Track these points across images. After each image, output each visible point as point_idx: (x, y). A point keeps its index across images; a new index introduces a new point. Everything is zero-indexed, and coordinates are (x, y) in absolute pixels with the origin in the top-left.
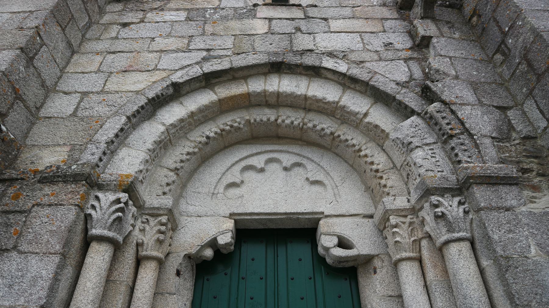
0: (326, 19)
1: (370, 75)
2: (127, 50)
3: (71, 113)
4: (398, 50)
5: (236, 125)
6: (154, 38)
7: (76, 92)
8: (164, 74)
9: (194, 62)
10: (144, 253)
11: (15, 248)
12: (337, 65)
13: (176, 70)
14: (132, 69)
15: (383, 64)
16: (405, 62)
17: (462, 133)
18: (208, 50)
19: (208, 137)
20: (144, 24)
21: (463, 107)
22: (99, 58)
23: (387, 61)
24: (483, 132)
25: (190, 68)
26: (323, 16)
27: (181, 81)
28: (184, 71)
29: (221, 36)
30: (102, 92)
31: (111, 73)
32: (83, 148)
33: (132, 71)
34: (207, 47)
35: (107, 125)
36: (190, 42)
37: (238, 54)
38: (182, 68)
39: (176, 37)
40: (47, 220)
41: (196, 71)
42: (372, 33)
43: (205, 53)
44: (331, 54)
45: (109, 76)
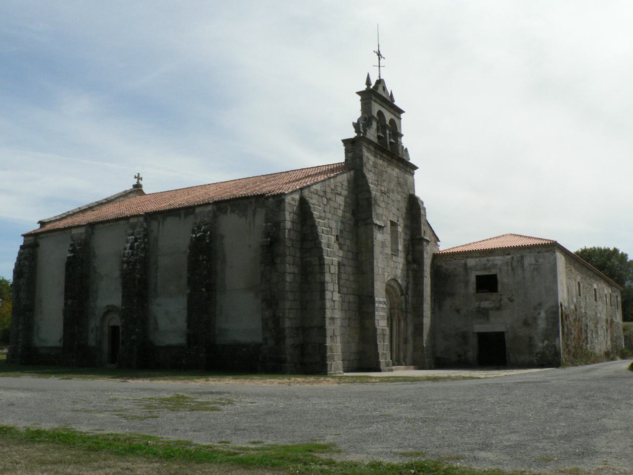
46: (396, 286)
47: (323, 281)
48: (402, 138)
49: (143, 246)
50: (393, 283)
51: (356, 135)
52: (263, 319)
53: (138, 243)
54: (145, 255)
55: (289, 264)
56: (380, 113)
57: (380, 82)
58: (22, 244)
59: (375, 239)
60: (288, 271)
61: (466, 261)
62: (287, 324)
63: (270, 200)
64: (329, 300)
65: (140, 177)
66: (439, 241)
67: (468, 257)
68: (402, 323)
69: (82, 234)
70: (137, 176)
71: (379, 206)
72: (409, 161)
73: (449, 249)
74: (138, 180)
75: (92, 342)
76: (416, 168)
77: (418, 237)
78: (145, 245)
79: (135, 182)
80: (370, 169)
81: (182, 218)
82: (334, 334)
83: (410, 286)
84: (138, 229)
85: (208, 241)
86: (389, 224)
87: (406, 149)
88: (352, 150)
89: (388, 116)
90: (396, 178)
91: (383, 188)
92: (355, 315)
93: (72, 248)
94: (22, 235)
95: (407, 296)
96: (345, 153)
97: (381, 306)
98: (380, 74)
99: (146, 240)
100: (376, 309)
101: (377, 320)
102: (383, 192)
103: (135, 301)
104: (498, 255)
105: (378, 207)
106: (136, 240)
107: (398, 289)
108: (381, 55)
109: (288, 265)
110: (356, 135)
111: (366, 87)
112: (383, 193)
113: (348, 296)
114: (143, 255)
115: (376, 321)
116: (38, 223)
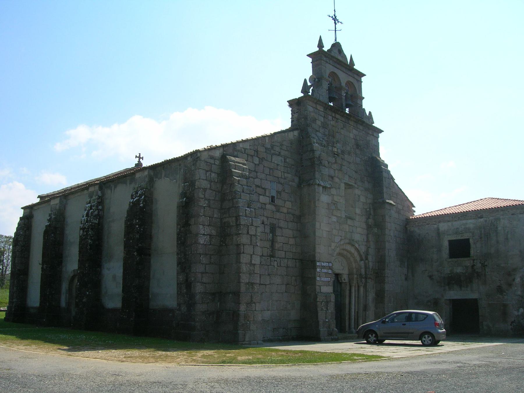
18: (341, 236)
46: (353, 250)
47: (239, 243)
48: (363, 101)
49: (96, 213)
50: (349, 247)
51: (302, 95)
52: (178, 284)
53: (92, 210)
54: (99, 222)
55: (204, 225)
56: (333, 75)
57: (337, 46)
58: (22, 216)
59: (318, 200)
60: (202, 232)
61: (438, 226)
62: (199, 288)
63: (189, 158)
64: (246, 264)
65: (141, 156)
66: (414, 207)
67: (440, 222)
68: (362, 289)
69: (57, 204)
70: (138, 156)
71: (325, 167)
72: (373, 125)
73: (423, 214)
74: (139, 159)
75: (63, 304)
76: (381, 131)
77: (381, 201)
78: (98, 212)
79: (136, 161)
80: (318, 130)
81: (128, 184)
82: (252, 301)
83: (372, 251)
84: (94, 198)
85: (141, 205)
86: (343, 186)
87: (370, 113)
88: (298, 111)
89: (344, 78)
90: (353, 141)
91: (335, 150)
92: (296, 280)
93: (96, 222)
94: (22, 208)
96: (292, 114)
97: (325, 271)
98: (336, 38)
99: (100, 207)
101: (320, 286)
102: (336, 153)
103: (87, 265)
104: (471, 219)
105: (324, 167)
106: (91, 208)
107: (356, 254)
108: (337, 20)
109: (201, 227)
110: (302, 95)
111: (317, 49)
112: (335, 155)
113: (286, 261)
114: (97, 222)
115: (317, 287)
116: (38, 198)
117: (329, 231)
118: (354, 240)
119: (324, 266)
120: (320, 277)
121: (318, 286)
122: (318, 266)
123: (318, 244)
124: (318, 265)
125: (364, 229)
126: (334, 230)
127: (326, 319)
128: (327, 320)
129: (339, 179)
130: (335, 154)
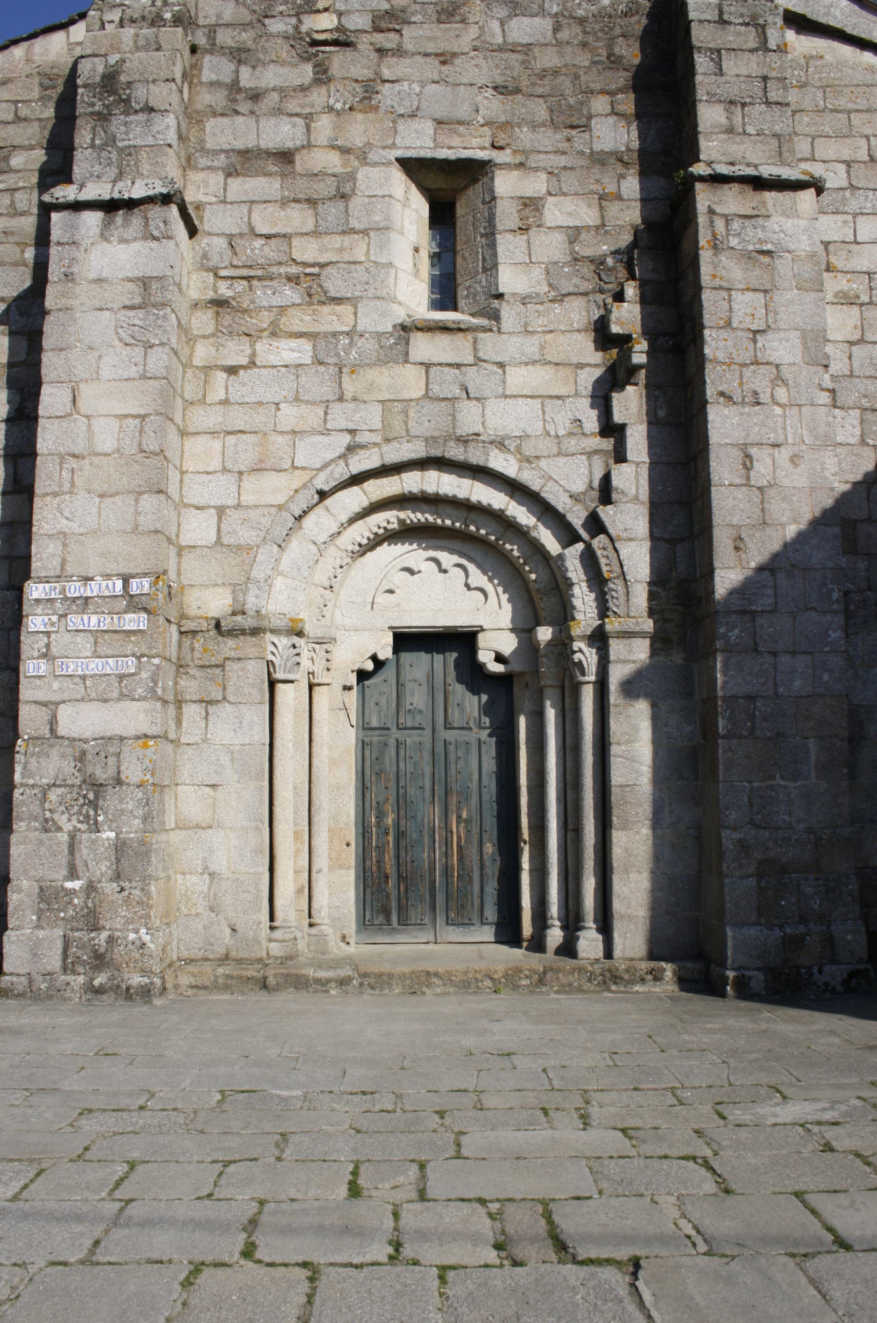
0: (501, 365)
1: (542, 481)
2: (247, 428)
3: (214, 539)
4: (584, 434)
5: (390, 527)
6: (277, 404)
7: (209, 507)
8: (305, 476)
9: (337, 454)
10: (316, 681)
11: (224, 698)
12: (505, 463)
13: (317, 470)
14: (263, 466)
15: (561, 460)
16: (589, 458)
17: (618, 577)
18: (352, 432)
19: (360, 545)
20: (257, 370)
21: (630, 543)
22: (217, 445)
23: (567, 455)
24: (639, 577)
25: (333, 465)
26: (499, 359)
27: (326, 488)
28: (328, 471)
29: (365, 402)
30: (238, 506)
31: (241, 473)
32: (243, 587)
33: (266, 470)
34: (352, 426)
35: (260, 557)
36: (326, 413)
37: (388, 440)
38: (326, 466)
39: (307, 402)
40: (241, 674)
41: (341, 472)
42: (558, 397)
43: (346, 439)
44: (500, 444)
45: (240, 480)
71: (152, 110)
95: (599, 542)
100: (30, 646)
101: (51, 706)
117: (143, 417)
118: (478, 435)
119: (87, 598)
120: (54, 658)
121: (36, 702)
122: (37, 601)
123: (55, 494)
124: (35, 595)
125: (580, 366)
126: (282, 406)
127: (73, 874)
128: (76, 885)
129: (345, 151)
130: (315, 43)
